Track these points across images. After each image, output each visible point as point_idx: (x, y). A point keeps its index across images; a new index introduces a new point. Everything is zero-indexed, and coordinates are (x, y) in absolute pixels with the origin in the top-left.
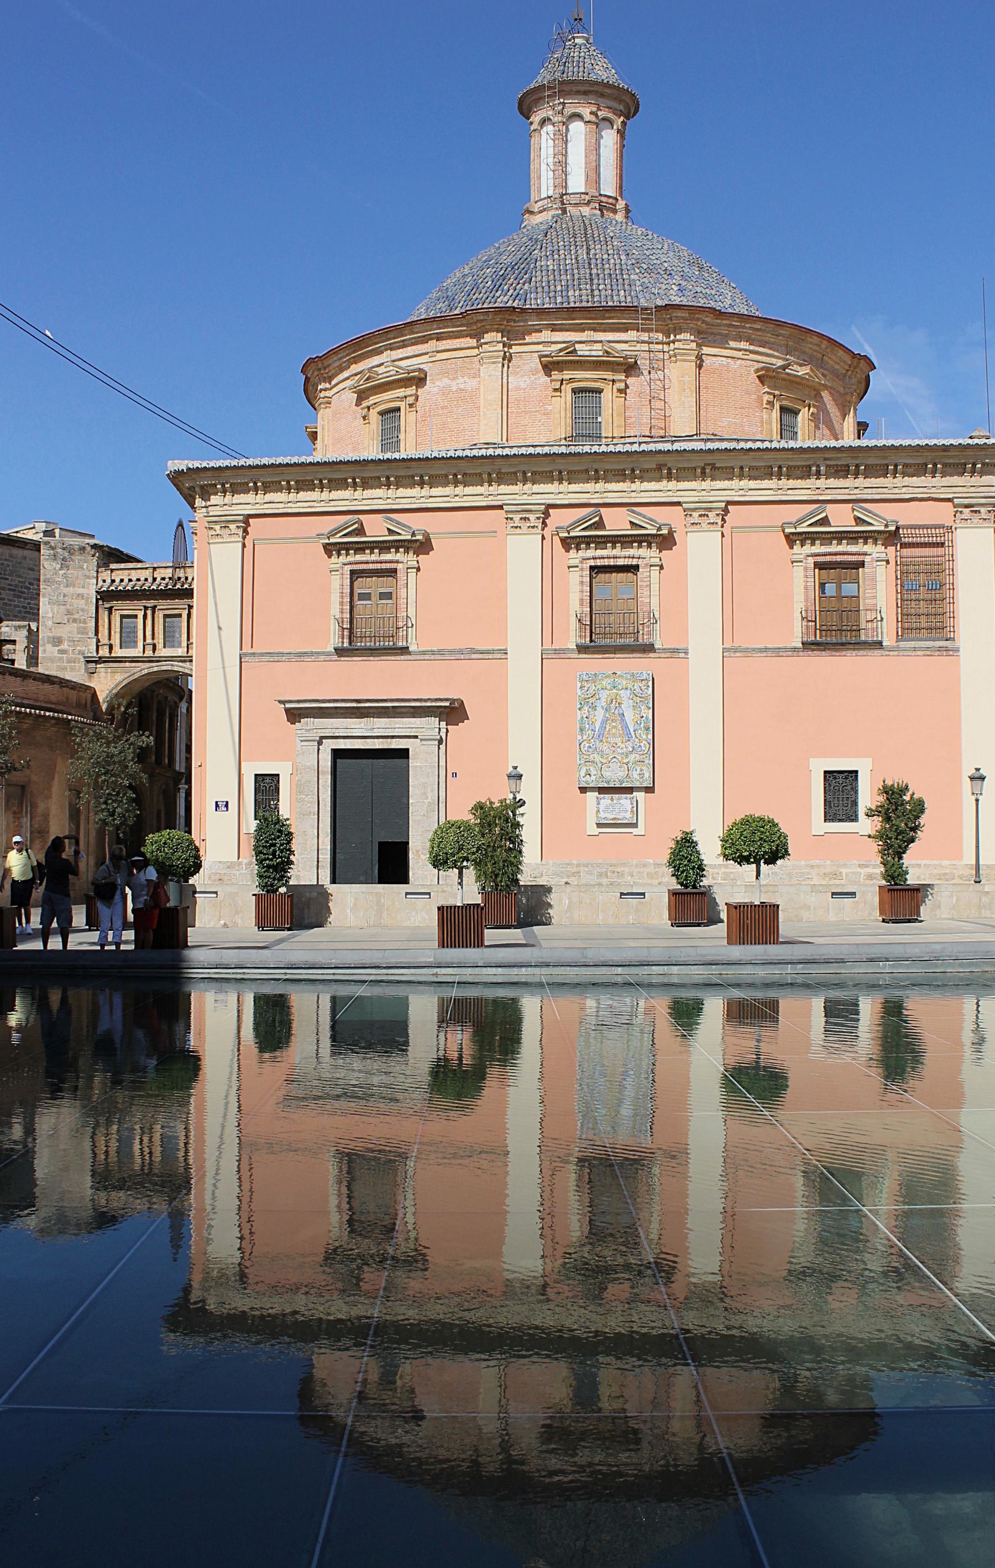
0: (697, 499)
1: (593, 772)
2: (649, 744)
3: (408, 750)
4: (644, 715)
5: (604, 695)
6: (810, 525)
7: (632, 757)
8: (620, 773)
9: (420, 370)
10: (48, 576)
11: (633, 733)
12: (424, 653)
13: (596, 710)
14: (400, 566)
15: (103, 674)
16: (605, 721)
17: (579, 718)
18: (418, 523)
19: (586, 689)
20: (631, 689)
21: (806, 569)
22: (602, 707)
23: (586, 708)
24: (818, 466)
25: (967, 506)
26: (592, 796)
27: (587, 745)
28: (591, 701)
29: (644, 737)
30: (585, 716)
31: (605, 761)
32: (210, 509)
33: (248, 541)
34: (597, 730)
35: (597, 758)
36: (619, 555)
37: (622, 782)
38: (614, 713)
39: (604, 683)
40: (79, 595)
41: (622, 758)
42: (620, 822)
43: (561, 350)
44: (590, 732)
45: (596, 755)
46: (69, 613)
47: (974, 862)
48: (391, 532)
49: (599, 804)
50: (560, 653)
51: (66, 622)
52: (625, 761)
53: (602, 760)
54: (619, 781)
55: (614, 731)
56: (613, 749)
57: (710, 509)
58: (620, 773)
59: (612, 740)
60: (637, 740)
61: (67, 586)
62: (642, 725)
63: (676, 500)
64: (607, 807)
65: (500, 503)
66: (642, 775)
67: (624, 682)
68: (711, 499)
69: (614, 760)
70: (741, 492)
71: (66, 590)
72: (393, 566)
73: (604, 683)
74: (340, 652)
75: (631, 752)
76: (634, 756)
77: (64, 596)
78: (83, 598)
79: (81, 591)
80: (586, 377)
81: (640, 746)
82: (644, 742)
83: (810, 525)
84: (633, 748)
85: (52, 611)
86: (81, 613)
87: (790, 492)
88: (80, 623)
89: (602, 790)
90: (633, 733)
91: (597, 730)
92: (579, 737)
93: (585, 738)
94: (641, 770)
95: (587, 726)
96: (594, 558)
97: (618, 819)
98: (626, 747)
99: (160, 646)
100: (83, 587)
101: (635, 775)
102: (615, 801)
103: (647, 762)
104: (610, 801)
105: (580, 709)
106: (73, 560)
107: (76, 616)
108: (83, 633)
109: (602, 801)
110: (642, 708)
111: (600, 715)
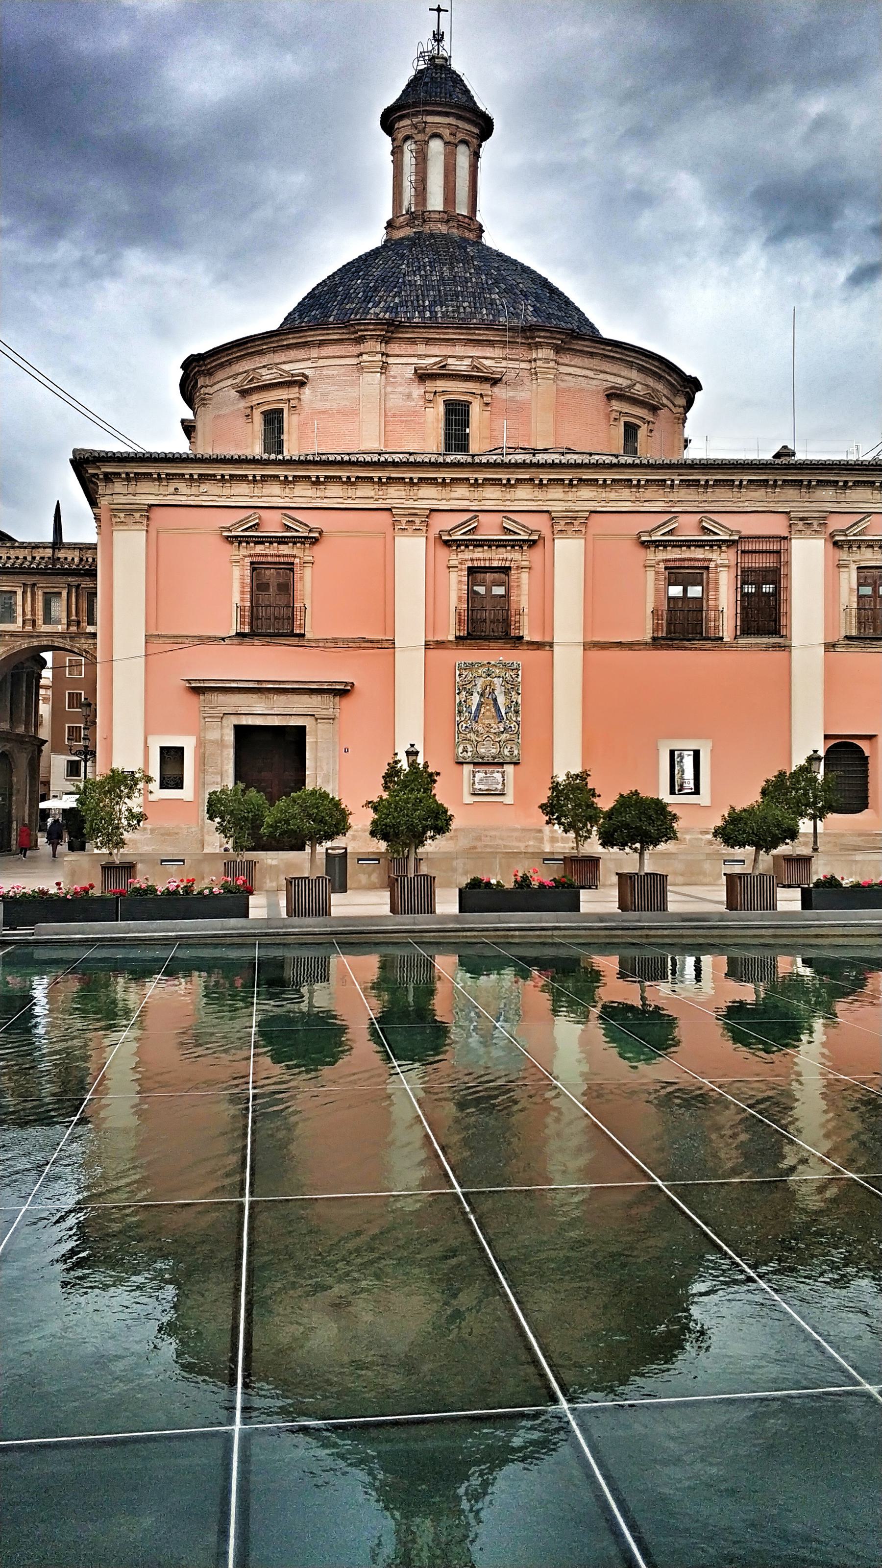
0: (564, 509)
1: (470, 749)
3: (305, 727)
5: (480, 682)
6: (663, 535)
7: (504, 736)
9: (303, 375)
12: (317, 640)
14: (297, 561)
16: (480, 705)
17: (457, 701)
18: (314, 520)
21: (657, 573)
23: (464, 693)
24: (673, 481)
25: (802, 519)
26: (467, 769)
28: (468, 687)
29: (514, 719)
31: (479, 740)
32: (115, 497)
33: (153, 533)
35: (473, 736)
36: (497, 557)
37: (494, 758)
43: (435, 364)
45: (472, 734)
47: (812, 831)
48: (288, 528)
49: (474, 777)
50: (440, 645)
52: (498, 740)
55: (488, 713)
57: (575, 518)
63: (545, 509)
64: (481, 780)
65: (389, 506)
67: (498, 671)
68: (577, 509)
70: (603, 504)
72: (291, 560)
74: (240, 635)
75: (502, 732)
76: (505, 735)
80: (457, 389)
83: (663, 535)
87: (646, 504)
89: (475, 764)
92: (458, 719)
96: (472, 560)
99: (40, 621)
101: (506, 752)
105: (458, 694)
109: (477, 775)
111: (476, 699)
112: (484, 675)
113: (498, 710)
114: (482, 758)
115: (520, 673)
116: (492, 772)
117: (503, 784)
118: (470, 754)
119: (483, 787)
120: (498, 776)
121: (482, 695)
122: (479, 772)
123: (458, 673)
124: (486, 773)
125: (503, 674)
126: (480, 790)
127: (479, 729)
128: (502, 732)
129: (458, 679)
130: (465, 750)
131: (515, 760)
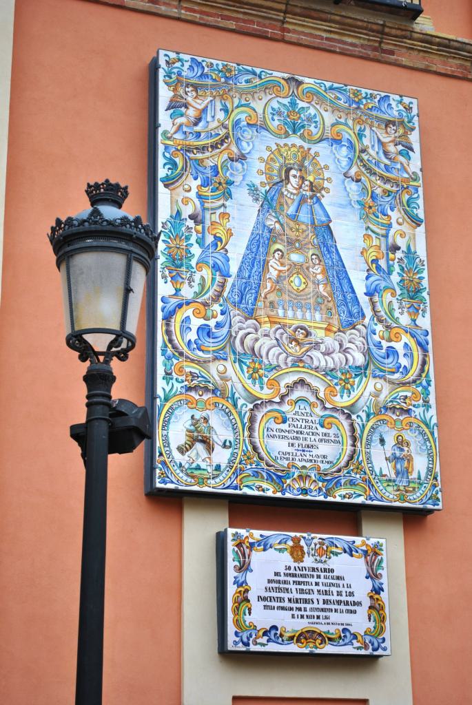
1: (221, 430)
2: (423, 346)
4: (401, 242)
7: (368, 390)
8: (324, 449)
11: (364, 300)
13: (229, 195)
16: (261, 243)
19: (191, 112)
20: (351, 146)
22: (253, 190)
27: (196, 322)
29: (405, 320)
30: (187, 211)
31: (265, 393)
34: (234, 270)
35: (234, 375)
37: (330, 480)
38: (294, 218)
39: (259, 106)
41: (331, 390)
42: (329, 649)
44: (207, 273)
45: (230, 368)
52: (343, 401)
53: (255, 390)
54: (322, 476)
55: (296, 281)
56: (295, 350)
58: (324, 449)
59: (294, 317)
60: (379, 328)
62: (395, 278)
64: (276, 583)
66: (400, 460)
67: (329, 118)
69: (299, 393)
73: (259, 106)
75: (361, 371)
81: (391, 352)
82: (406, 338)
84: (368, 353)
90: (364, 300)
91: (234, 270)
93: (187, 292)
94: (401, 443)
95: (196, 250)
97: (325, 638)
98: (345, 351)
101: (380, 461)
102: (308, 562)
103: (418, 412)
104: (286, 559)
109: (257, 557)
110: (395, 215)
112: (275, 124)
113: (338, 274)
114: (278, 478)
115: (414, 138)
116: (325, 551)
117: (376, 608)
118: (221, 456)
119: (290, 623)
120: (351, 569)
121: (269, 202)
122: (265, 545)
123: (165, 94)
124: (297, 552)
125: (348, 134)
126: (272, 632)
127: (264, 344)
128: (361, 371)
129: (165, 120)
130: (200, 437)
131: (415, 501)
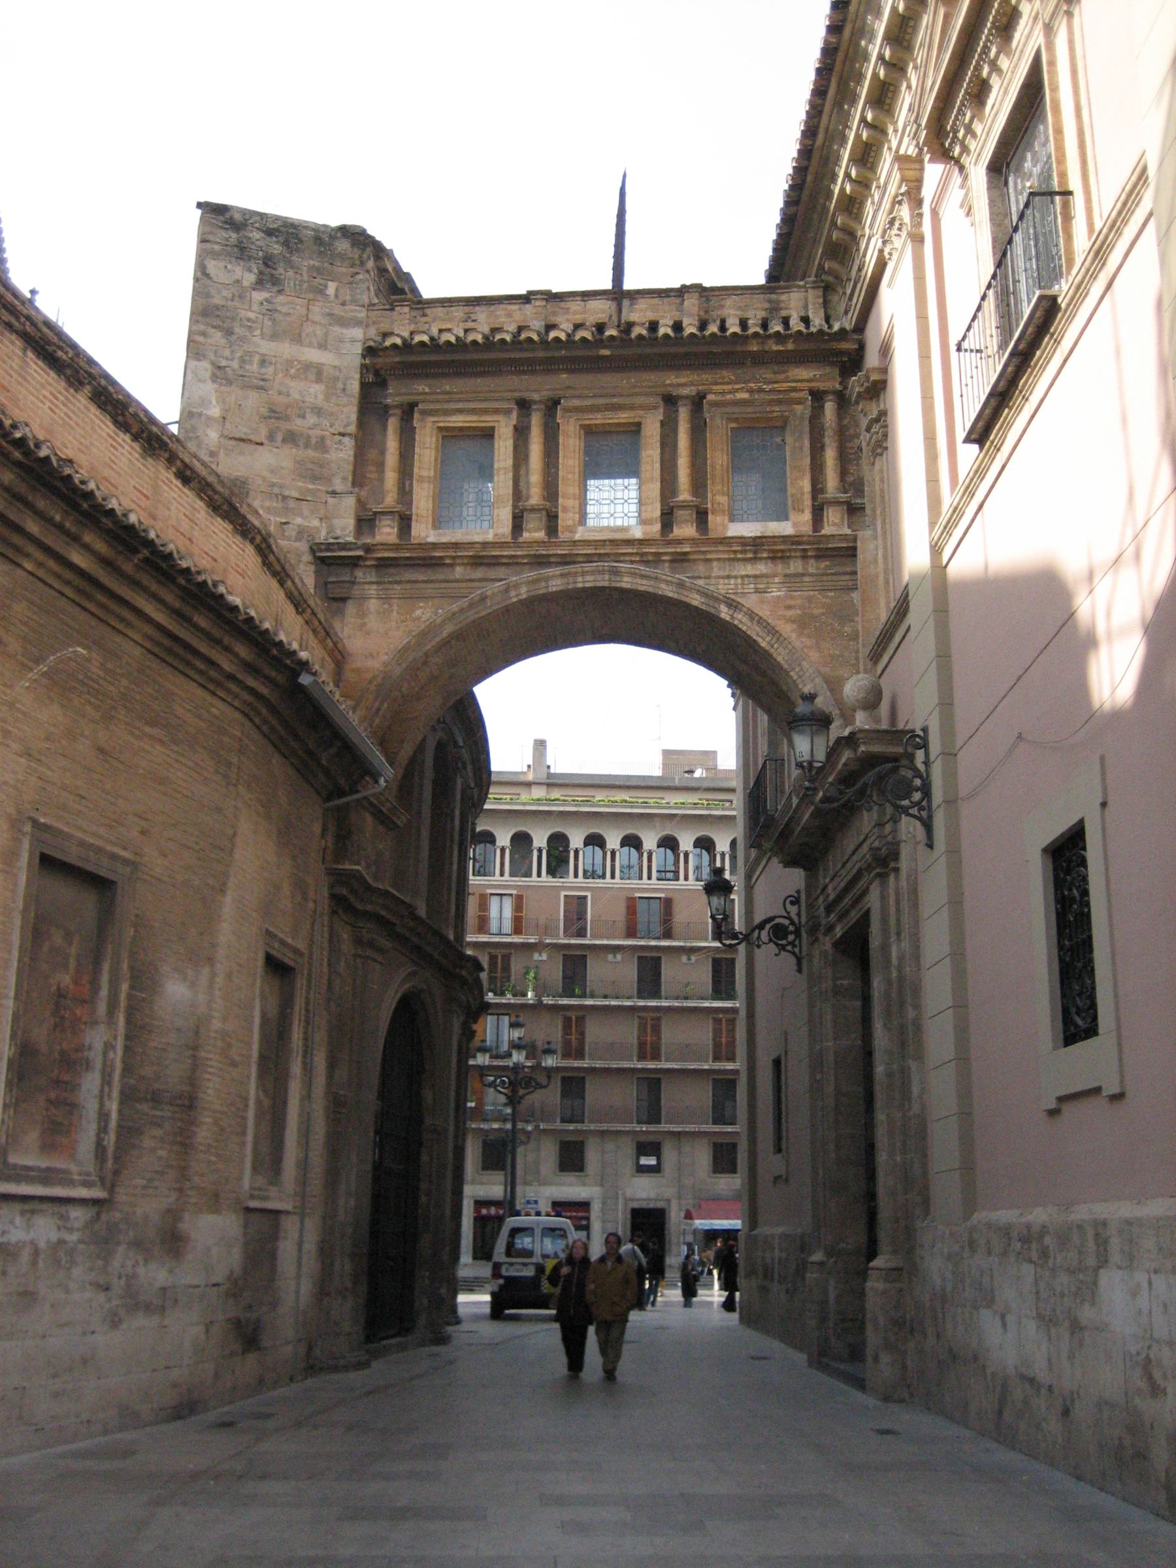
10: (217, 301)
15: (373, 604)
40: (307, 367)
46: (274, 414)
51: (262, 436)
61: (274, 337)
71: (266, 347)
77: (263, 362)
78: (318, 380)
79: (314, 355)
85: (222, 400)
86: (312, 419)
88: (307, 445)
100: (323, 346)
106: (290, 264)
107: (298, 424)
108: (315, 478)
